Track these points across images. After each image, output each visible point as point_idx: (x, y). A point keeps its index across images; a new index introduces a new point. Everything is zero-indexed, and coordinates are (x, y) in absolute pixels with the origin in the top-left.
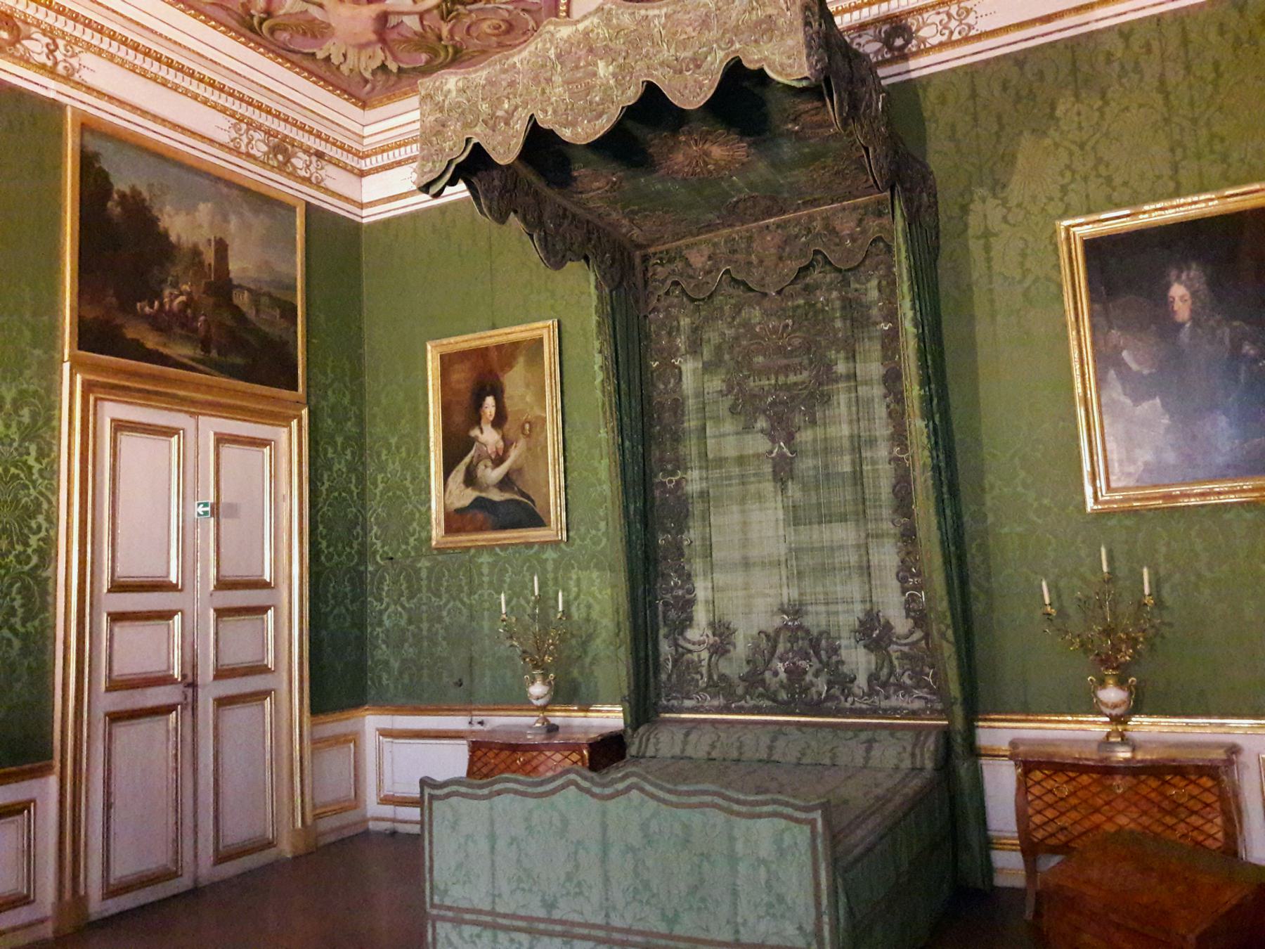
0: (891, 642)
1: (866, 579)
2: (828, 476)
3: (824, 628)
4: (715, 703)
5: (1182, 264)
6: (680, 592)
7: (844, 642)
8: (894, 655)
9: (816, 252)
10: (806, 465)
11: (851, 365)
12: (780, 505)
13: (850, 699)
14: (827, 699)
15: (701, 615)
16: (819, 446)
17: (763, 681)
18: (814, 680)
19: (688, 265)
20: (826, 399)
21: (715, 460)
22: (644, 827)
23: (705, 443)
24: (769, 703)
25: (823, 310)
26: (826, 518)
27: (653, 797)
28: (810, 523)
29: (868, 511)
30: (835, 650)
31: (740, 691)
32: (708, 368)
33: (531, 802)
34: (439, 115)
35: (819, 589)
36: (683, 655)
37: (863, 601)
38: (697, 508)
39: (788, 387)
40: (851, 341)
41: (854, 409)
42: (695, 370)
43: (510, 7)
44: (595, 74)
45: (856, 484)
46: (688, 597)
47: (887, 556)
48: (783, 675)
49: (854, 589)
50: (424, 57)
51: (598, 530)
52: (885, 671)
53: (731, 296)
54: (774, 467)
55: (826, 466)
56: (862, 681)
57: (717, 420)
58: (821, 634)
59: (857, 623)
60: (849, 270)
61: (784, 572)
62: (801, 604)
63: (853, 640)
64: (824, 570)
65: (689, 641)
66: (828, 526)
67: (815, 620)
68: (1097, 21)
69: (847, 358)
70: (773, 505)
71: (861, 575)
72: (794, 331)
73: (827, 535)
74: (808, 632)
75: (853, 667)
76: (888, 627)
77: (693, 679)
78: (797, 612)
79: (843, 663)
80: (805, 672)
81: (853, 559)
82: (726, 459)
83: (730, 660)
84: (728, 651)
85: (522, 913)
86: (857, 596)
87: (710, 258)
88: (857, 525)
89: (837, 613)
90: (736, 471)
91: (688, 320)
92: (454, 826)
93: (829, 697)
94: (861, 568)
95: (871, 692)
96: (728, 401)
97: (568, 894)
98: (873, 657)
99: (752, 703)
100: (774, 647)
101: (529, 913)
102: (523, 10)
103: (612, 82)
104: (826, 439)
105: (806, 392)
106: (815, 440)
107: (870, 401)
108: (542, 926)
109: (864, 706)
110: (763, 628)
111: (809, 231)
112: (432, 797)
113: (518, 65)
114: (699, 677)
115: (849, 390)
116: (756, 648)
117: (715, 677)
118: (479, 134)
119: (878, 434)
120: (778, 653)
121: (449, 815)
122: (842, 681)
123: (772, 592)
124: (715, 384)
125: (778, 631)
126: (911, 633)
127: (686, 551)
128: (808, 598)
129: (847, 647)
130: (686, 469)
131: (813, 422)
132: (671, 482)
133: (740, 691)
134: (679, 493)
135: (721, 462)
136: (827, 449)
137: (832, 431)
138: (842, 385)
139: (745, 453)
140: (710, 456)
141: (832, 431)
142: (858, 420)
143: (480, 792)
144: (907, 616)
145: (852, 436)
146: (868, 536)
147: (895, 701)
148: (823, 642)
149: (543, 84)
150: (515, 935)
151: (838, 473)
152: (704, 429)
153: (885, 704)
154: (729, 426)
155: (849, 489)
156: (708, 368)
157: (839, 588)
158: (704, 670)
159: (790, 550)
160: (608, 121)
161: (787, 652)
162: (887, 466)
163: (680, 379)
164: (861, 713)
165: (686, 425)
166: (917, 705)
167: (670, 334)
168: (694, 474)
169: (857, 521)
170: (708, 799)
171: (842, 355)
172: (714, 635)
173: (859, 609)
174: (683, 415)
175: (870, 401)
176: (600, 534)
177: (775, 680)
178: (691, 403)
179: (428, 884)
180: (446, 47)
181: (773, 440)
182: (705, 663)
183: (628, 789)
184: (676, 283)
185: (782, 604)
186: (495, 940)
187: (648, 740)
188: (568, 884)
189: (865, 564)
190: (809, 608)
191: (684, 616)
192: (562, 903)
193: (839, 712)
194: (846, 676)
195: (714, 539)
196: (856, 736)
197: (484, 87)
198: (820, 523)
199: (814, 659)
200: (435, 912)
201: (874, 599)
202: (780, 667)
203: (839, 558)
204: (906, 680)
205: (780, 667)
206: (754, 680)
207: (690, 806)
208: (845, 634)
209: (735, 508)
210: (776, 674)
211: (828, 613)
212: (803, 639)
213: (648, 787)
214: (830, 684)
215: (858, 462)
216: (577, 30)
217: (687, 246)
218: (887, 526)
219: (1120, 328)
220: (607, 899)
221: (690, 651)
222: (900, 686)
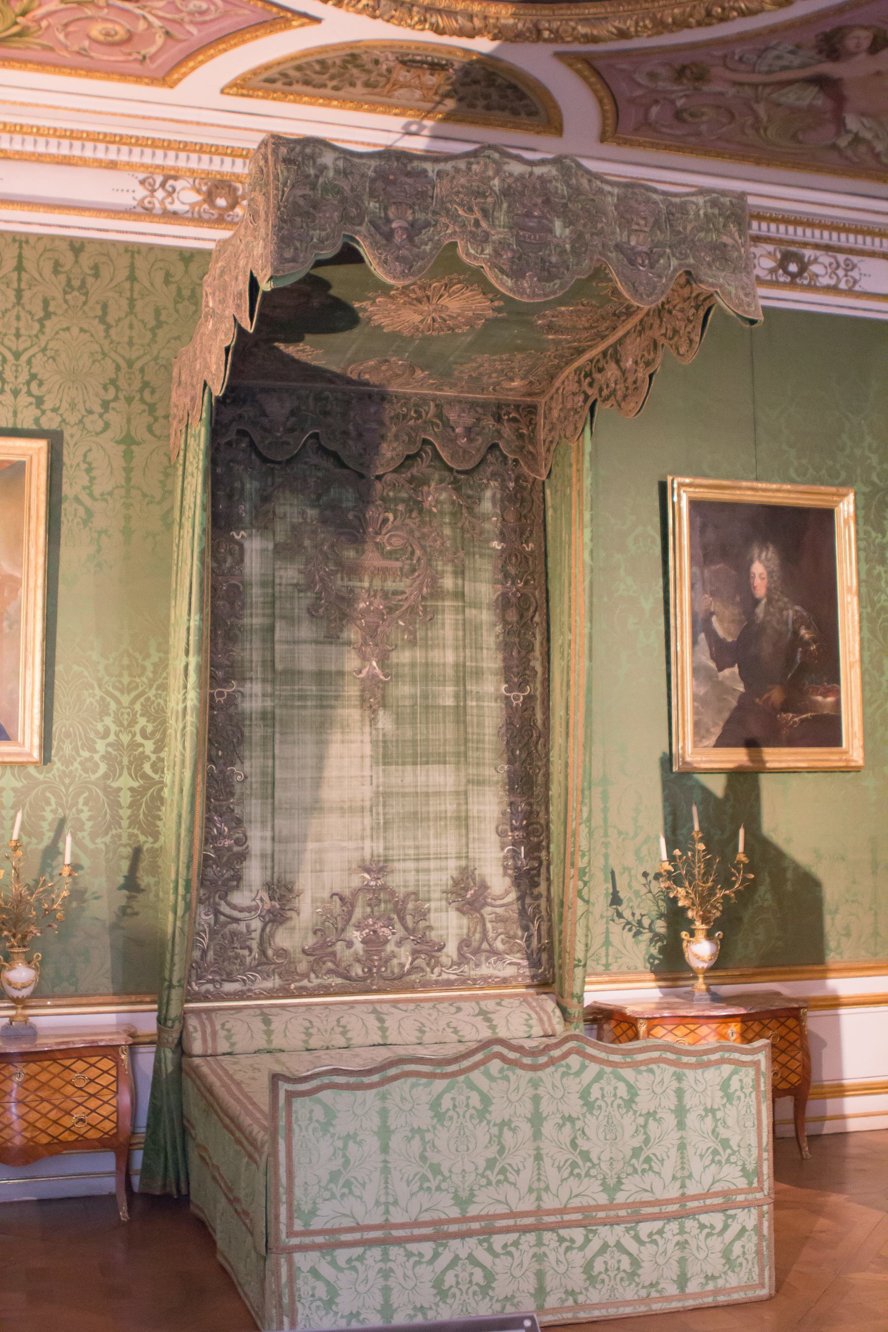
0: (486, 904)
1: (463, 831)
2: (427, 707)
3: (411, 889)
4: (269, 984)
5: (764, 544)
6: (227, 843)
7: (433, 905)
8: (488, 918)
9: (425, 442)
10: (403, 690)
11: (460, 582)
12: (367, 738)
13: (437, 970)
14: (409, 972)
15: (254, 873)
16: (418, 671)
17: (334, 954)
18: (396, 949)
19: (264, 414)
20: (431, 618)
21: (285, 672)
22: (585, 1095)
23: (273, 649)
24: (339, 981)
25: (430, 511)
26: (423, 757)
27: (593, 1059)
28: (404, 764)
29: (470, 753)
30: (424, 915)
31: (303, 967)
32: (282, 552)
33: (440, 1084)
34: (308, 192)
35: (410, 843)
36: (225, 925)
37: (459, 858)
38: (256, 733)
39: (386, 595)
40: (461, 554)
41: (460, 633)
42: (264, 551)
43: (157, 23)
45: (458, 722)
46: (236, 849)
47: (490, 806)
48: (359, 947)
49: (451, 842)
51: (94, 751)
52: (478, 936)
53: (317, 467)
54: (363, 690)
55: (425, 696)
56: (451, 949)
57: (291, 620)
58: (407, 895)
59: (450, 882)
60: (459, 472)
61: (367, 821)
62: (386, 861)
63: (444, 903)
64: (416, 818)
65: (234, 907)
66: (425, 767)
67: (401, 879)
69: (455, 574)
70: (358, 737)
71: (459, 827)
72: (395, 528)
73: (421, 779)
74: (393, 893)
75: (443, 932)
76: (484, 886)
77: (237, 957)
78: (381, 870)
79: (430, 928)
80: (387, 941)
81: (450, 806)
82: (301, 672)
83: (293, 929)
84: (290, 918)
85: (426, 1217)
86: (452, 850)
87: (292, 413)
88: (458, 770)
89: (428, 871)
90: (312, 689)
91: (256, 484)
92: (326, 1126)
93: (414, 969)
94: (458, 818)
95: (462, 959)
96: (306, 600)
97: (489, 1183)
98: (465, 921)
99: (316, 982)
100: (350, 913)
101: (435, 1215)
102: (167, 33)
103: (568, 246)
104: (427, 665)
105: (406, 605)
106: (413, 665)
107: (478, 627)
108: (453, 1228)
109: (453, 977)
110: (337, 890)
111: (419, 416)
112: (290, 1095)
114: (246, 952)
115: (456, 610)
116: (327, 915)
117: (270, 952)
119: (485, 665)
120: (354, 920)
121: (319, 1113)
122: (428, 949)
123: (352, 845)
124: (290, 574)
125: (355, 893)
126: (507, 893)
127: (238, 789)
128: (394, 853)
129: (436, 910)
130: (243, 680)
131: (413, 643)
132: (221, 694)
133: (303, 967)
134: (232, 710)
135: (292, 675)
136: (428, 675)
137: (435, 655)
138: (447, 603)
139: (327, 667)
140: (279, 667)
141: (435, 655)
142: (464, 647)
143: (367, 1080)
144: (505, 874)
145: (457, 665)
146: (468, 782)
147: (485, 970)
148: (410, 906)
150: (413, 1247)
151: (439, 707)
152: (272, 629)
153: (475, 973)
154: (305, 631)
155: (450, 726)
156: (282, 552)
157: (432, 842)
158: (254, 945)
159: (377, 793)
161: (366, 918)
162: (493, 704)
163: (242, 560)
164: (448, 984)
165: (246, 621)
166: (509, 971)
167: (230, 497)
168: (257, 688)
169: (458, 763)
170: (656, 1054)
171: (449, 568)
172: (272, 898)
173: (452, 864)
174: (242, 608)
175: (478, 627)
176: (97, 757)
177: (348, 952)
178: (256, 593)
179: (283, 1210)
181: (364, 658)
182: (256, 935)
183: (565, 1056)
184: (242, 433)
185: (363, 860)
186: (385, 1258)
187: (214, 1033)
188: (488, 1173)
189: (463, 814)
190: (396, 865)
191: (228, 874)
192: (482, 1196)
193: (426, 985)
194: (435, 944)
195: (277, 776)
196: (459, 1009)
198: (415, 763)
199: (398, 926)
200: (295, 1241)
201: (471, 855)
202: (356, 936)
203: (434, 806)
204: (499, 945)
205: (356, 936)
206: (321, 953)
207: (635, 1065)
208: (436, 895)
209: (309, 737)
210: (350, 944)
211: (417, 871)
212: (386, 902)
213: (590, 1050)
214: (415, 953)
215: (462, 696)
216: (531, 174)
217: (267, 391)
218: (488, 772)
219: (712, 594)
220: (539, 1180)
221: (237, 920)
222: (493, 952)
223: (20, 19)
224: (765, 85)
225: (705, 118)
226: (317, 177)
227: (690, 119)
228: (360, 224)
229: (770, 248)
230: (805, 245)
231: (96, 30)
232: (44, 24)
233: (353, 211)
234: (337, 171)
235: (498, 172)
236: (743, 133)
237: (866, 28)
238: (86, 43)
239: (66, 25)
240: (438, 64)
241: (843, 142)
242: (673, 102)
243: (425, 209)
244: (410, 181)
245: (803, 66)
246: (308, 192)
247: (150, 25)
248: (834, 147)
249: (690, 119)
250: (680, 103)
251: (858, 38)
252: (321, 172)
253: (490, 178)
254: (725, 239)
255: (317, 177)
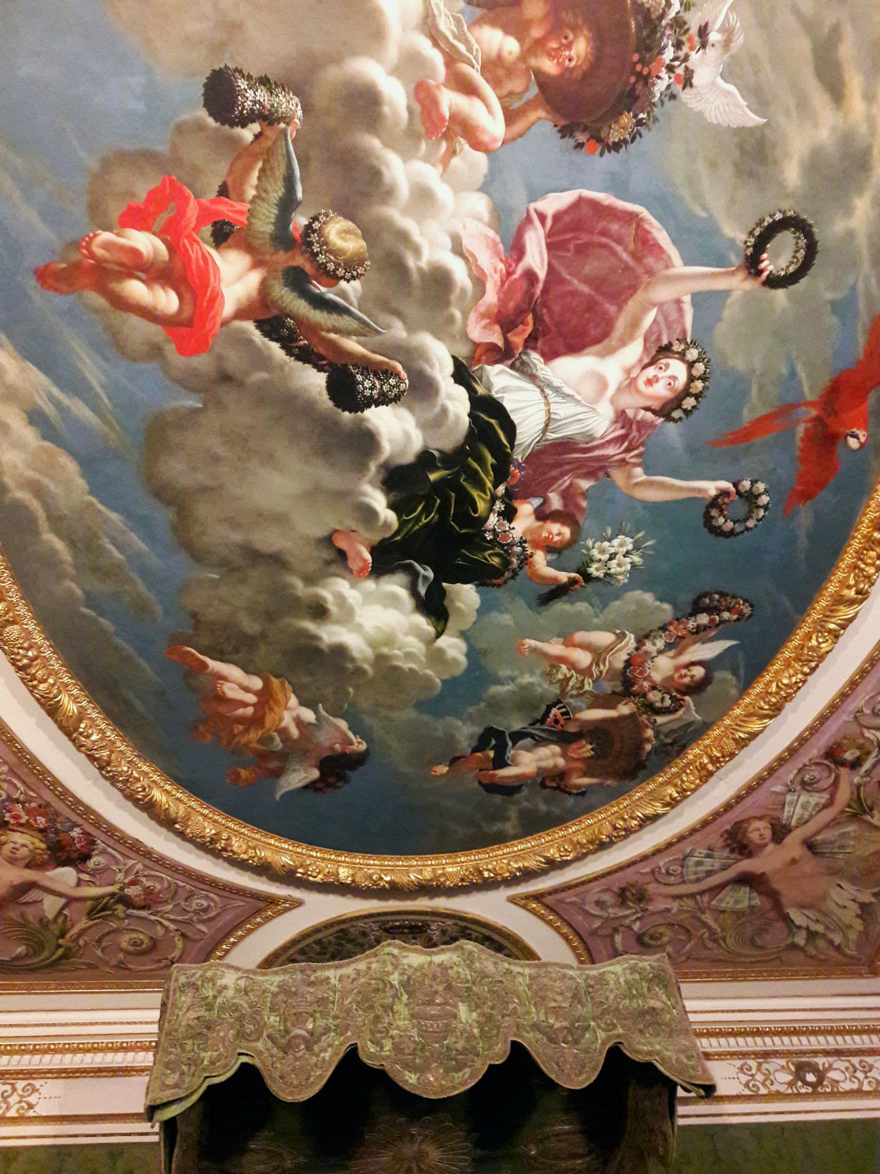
34: (202, 1012)
43: (172, 927)
44: (455, 1016)
50: (21, 949)
68: (729, 1115)
102: (183, 935)
103: (476, 1031)
113: (333, 981)
118: (262, 1053)
149: (380, 1011)
160: (472, 1076)
180: (60, 946)
197: (275, 995)
216: (430, 963)
223: (61, 941)
224: (702, 893)
225: (665, 939)
226: (215, 997)
227: (653, 942)
228: (258, 1040)
229: (783, 1062)
230: (815, 1053)
231: (124, 941)
232: (81, 942)
233: (250, 1028)
234: (238, 990)
235: (396, 967)
236: (706, 948)
237: (760, 818)
238: (121, 956)
239: (99, 941)
240: (416, 927)
241: (800, 939)
242: (629, 927)
243: (324, 1015)
244: (311, 990)
245: (724, 868)
246: (202, 1012)
247: (166, 929)
248: (794, 946)
249: (653, 942)
250: (636, 927)
251: (758, 830)
252: (220, 992)
253: (388, 974)
254: (653, 1003)
255: (215, 997)
